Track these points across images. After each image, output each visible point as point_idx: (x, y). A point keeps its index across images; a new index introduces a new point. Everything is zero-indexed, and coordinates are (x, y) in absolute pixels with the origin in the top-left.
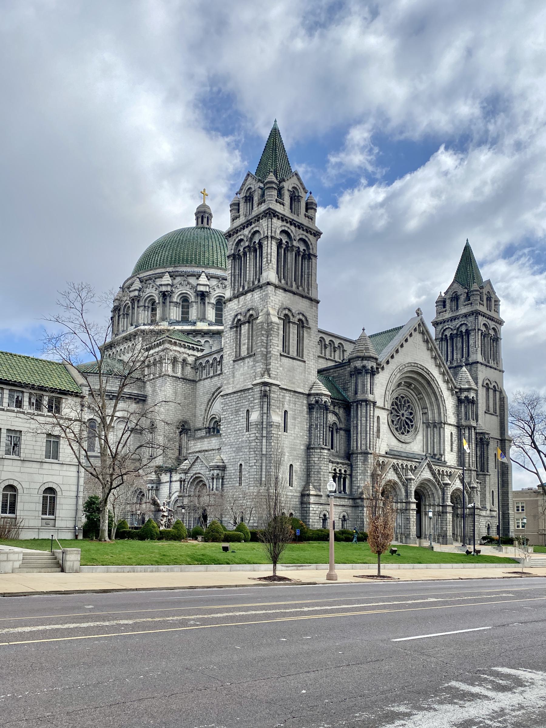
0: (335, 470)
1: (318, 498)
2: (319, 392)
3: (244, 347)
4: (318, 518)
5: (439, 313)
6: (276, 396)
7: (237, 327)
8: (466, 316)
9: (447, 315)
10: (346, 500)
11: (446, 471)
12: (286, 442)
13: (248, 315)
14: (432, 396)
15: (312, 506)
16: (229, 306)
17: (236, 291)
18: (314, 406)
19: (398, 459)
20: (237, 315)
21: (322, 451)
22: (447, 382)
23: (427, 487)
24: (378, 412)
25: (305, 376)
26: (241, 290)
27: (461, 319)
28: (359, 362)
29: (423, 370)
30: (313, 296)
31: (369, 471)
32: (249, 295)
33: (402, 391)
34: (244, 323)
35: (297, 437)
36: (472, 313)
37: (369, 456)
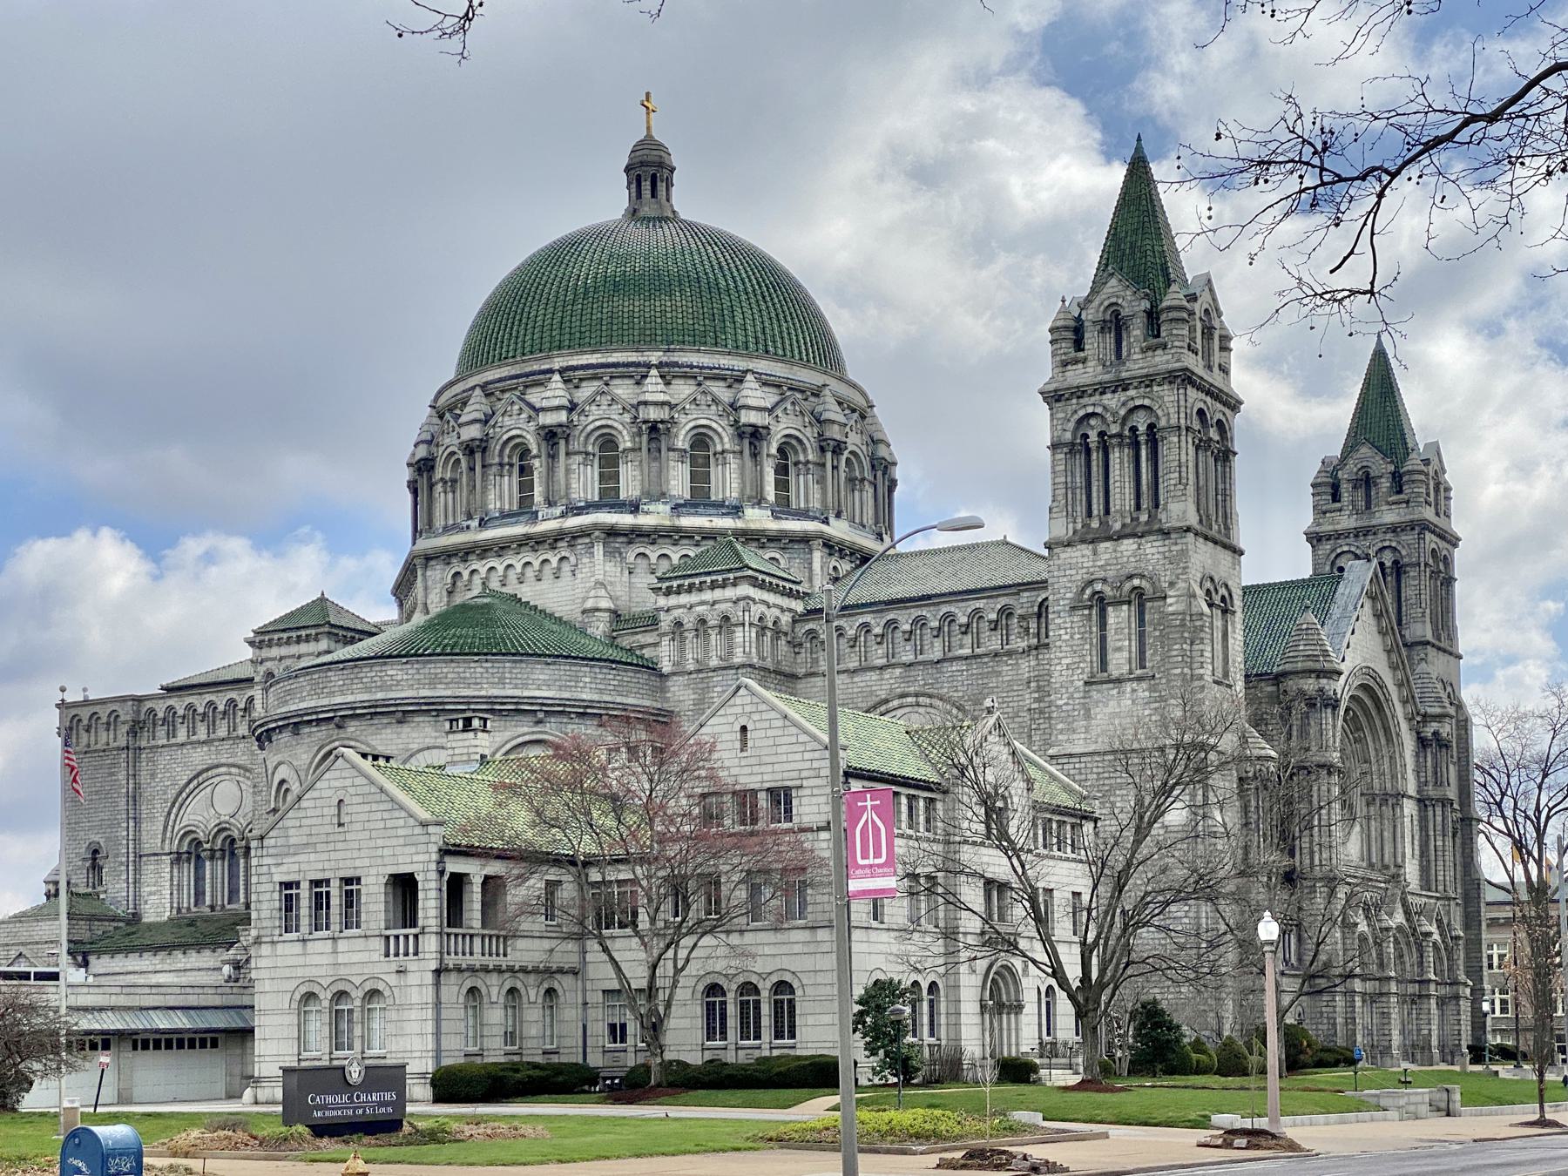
2: (1263, 752)
3: (1117, 655)
5: (1320, 512)
7: (1091, 607)
8: (1394, 529)
9: (1346, 521)
13: (1127, 586)
16: (1063, 556)
17: (1079, 526)
20: (1091, 582)
22: (1404, 702)
26: (1095, 524)
27: (1380, 536)
28: (1311, 681)
30: (1235, 543)
32: (1128, 545)
34: (1118, 603)
36: (1412, 526)
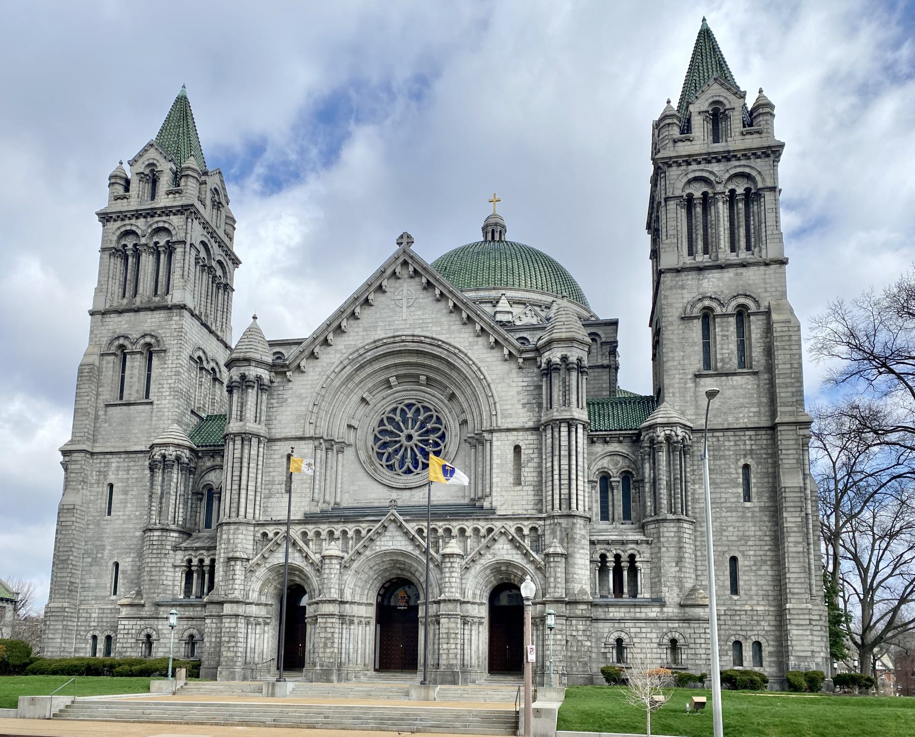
0: (190, 561)
1: (135, 608)
4: (134, 641)
6: (79, 466)
10: (199, 609)
11: (476, 530)
12: (108, 530)
14: (463, 384)
15: (123, 622)
18: (159, 464)
19: (315, 523)
21: (149, 534)
23: (412, 569)
24: (283, 448)
25: (150, 425)
29: (421, 342)
31: (222, 555)
33: (405, 393)
35: (129, 519)
37: (225, 528)
